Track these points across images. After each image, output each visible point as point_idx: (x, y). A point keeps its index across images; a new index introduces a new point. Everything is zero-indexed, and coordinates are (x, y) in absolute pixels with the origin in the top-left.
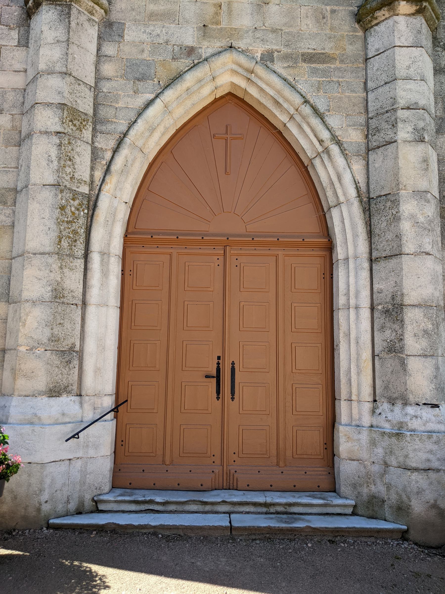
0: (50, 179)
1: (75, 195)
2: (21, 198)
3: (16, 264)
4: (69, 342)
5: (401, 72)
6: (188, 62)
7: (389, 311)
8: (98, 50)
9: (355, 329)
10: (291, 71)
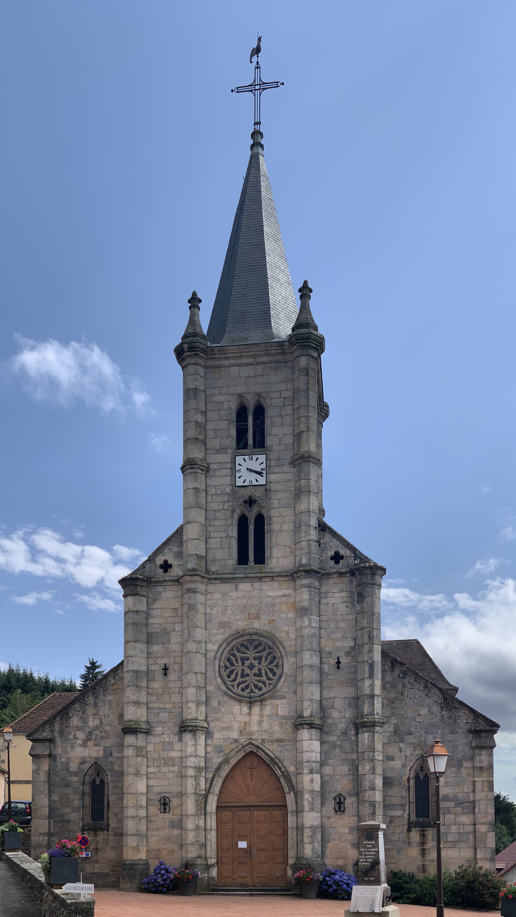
0: (193, 791)
1: (201, 795)
2: (184, 796)
3: (184, 818)
4: (202, 842)
5: (305, 749)
6: (236, 745)
7: (300, 829)
8: (205, 742)
9: (292, 835)
10: (271, 746)
